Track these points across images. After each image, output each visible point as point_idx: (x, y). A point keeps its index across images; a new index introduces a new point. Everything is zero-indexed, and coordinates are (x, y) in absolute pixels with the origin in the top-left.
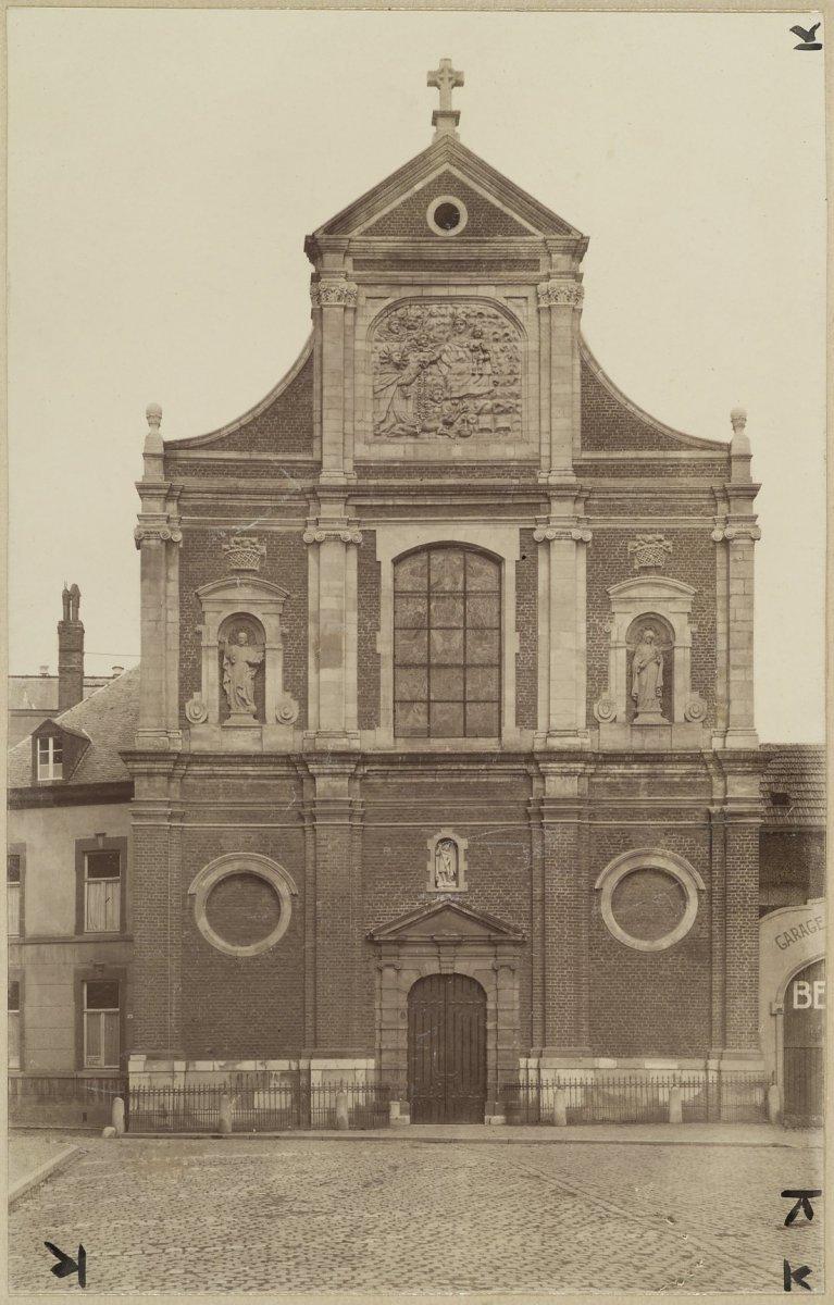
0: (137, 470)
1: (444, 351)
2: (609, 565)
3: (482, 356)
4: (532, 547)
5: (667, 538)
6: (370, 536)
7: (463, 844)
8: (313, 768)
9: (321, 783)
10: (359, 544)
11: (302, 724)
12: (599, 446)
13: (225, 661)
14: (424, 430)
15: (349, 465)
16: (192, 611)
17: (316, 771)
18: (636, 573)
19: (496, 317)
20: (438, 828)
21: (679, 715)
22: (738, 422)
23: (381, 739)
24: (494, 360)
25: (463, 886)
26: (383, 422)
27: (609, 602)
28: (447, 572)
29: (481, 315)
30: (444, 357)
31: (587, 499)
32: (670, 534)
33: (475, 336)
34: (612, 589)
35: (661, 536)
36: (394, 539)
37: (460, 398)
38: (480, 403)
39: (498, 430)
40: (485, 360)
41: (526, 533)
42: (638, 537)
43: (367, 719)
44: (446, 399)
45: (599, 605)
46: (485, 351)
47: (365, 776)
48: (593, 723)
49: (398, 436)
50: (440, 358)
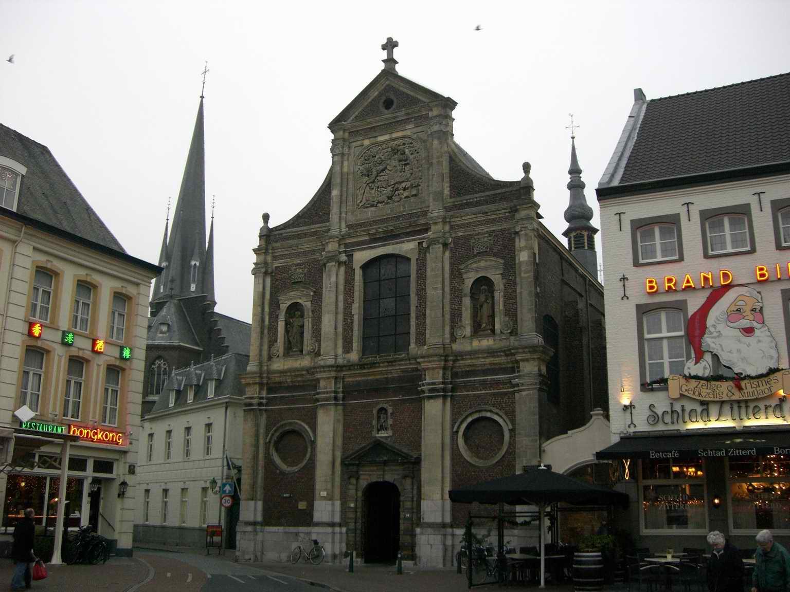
0: (256, 243)
1: (388, 164)
2: (461, 252)
3: (404, 163)
4: (423, 251)
5: (490, 236)
6: (350, 256)
7: (390, 411)
8: (319, 376)
9: (322, 384)
10: (345, 262)
11: (318, 354)
12: (459, 195)
13: (289, 326)
14: (379, 202)
15: (343, 225)
16: (275, 304)
17: (319, 377)
18: (475, 256)
19: (411, 143)
20: (377, 403)
21: (497, 326)
22: (527, 167)
23: (354, 356)
24: (410, 163)
25: (390, 433)
26: (360, 202)
27: (461, 274)
28: (387, 270)
29: (404, 144)
30: (388, 167)
31: (450, 222)
32: (490, 234)
33: (402, 154)
34: (462, 267)
35: (486, 235)
36: (362, 256)
37: (394, 184)
38: (403, 185)
39: (413, 196)
40: (405, 165)
41: (420, 244)
42: (476, 237)
43: (347, 349)
44: (389, 186)
45: (456, 275)
46: (406, 160)
47: (343, 378)
48: (453, 339)
49: (367, 207)
50: (386, 168)
